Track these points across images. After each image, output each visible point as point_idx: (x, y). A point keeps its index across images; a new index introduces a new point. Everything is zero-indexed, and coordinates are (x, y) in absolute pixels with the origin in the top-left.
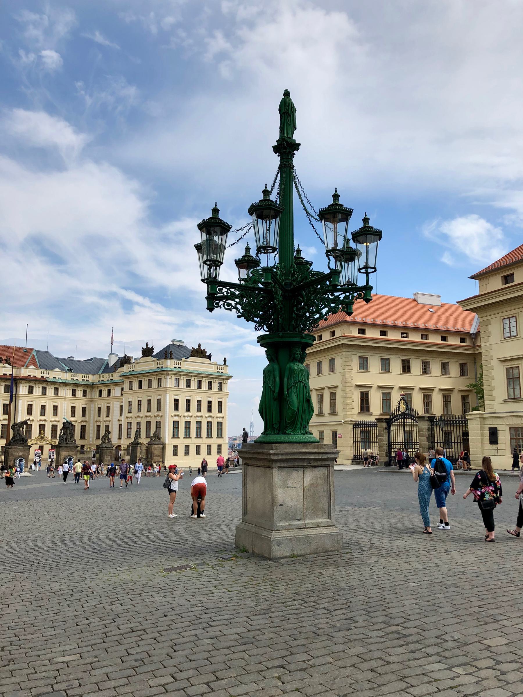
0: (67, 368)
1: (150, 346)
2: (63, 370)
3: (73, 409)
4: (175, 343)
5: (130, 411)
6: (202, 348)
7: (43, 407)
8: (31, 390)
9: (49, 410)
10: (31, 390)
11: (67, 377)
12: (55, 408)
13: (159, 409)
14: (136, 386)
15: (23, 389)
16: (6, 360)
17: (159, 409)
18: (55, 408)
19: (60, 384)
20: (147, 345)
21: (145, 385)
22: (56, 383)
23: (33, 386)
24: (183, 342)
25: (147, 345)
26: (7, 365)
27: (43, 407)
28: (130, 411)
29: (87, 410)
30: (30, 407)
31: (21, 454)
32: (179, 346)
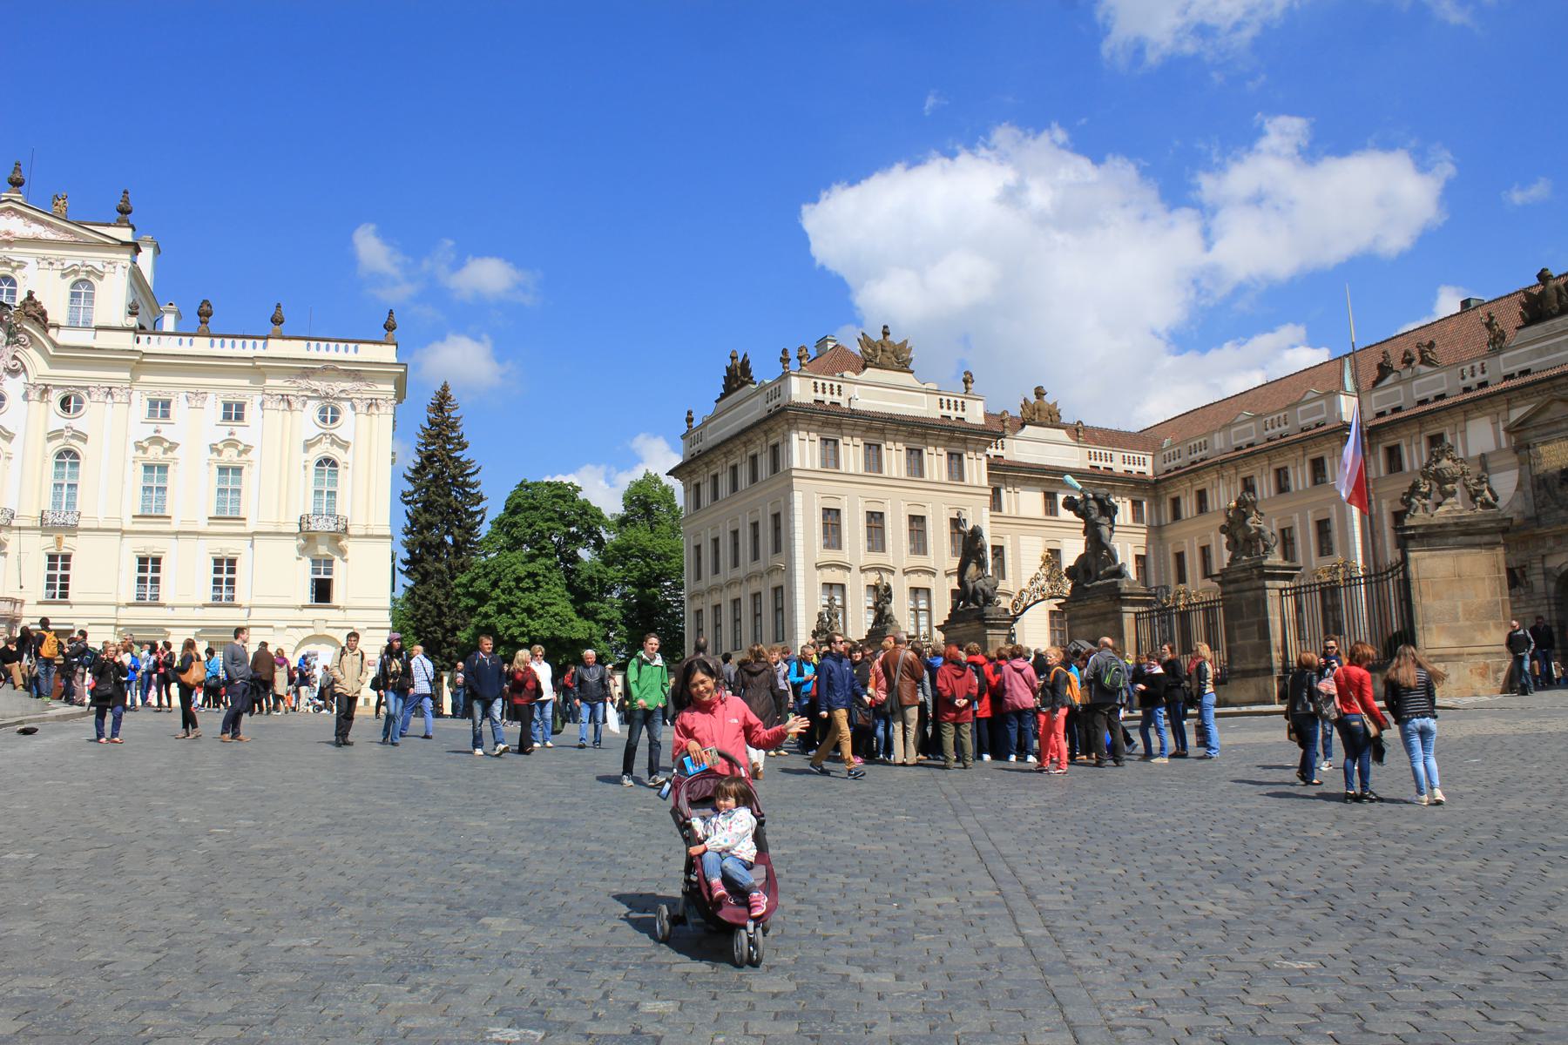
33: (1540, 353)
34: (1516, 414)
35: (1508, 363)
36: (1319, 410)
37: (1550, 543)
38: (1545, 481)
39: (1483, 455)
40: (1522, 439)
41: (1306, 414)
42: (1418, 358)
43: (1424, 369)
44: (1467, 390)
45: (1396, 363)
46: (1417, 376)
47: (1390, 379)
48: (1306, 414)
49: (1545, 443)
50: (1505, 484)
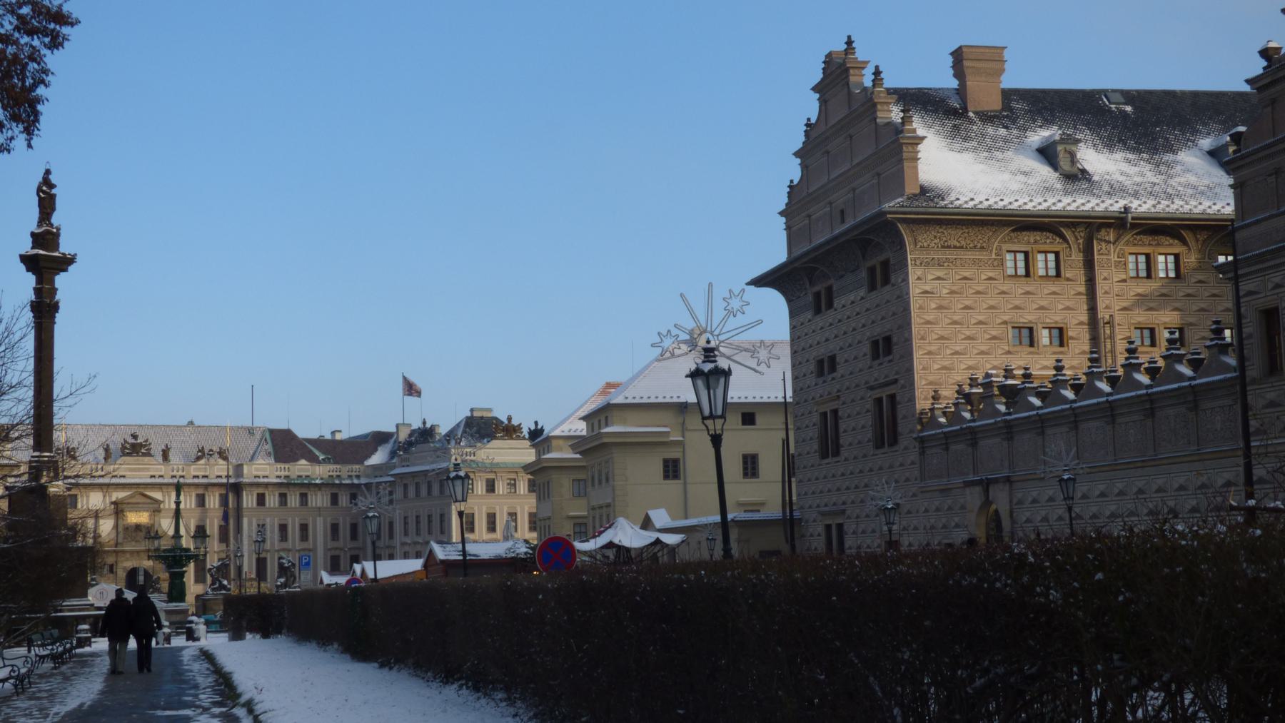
0: (322, 457)
1: (428, 426)
2: (313, 460)
3: (335, 528)
4: (475, 414)
5: (406, 534)
6: (515, 422)
7: (283, 528)
8: (261, 500)
9: (294, 532)
10: (261, 500)
11: (320, 472)
12: (304, 528)
13: (442, 532)
14: (412, 492)
15: (249, 500)
16: (220, 453)
17: (442, 532)
18: (304, 528)
19: (309, 485)
20: (424, 423)
21: (412, 492)
22: (302, 485)
23: (263, 495)
24: (490, 410)
25: (424, 423)
27: (283, 528)
28: (406, 534)
29: (360, 529)
32: (482, 418)
40: (118, 509)
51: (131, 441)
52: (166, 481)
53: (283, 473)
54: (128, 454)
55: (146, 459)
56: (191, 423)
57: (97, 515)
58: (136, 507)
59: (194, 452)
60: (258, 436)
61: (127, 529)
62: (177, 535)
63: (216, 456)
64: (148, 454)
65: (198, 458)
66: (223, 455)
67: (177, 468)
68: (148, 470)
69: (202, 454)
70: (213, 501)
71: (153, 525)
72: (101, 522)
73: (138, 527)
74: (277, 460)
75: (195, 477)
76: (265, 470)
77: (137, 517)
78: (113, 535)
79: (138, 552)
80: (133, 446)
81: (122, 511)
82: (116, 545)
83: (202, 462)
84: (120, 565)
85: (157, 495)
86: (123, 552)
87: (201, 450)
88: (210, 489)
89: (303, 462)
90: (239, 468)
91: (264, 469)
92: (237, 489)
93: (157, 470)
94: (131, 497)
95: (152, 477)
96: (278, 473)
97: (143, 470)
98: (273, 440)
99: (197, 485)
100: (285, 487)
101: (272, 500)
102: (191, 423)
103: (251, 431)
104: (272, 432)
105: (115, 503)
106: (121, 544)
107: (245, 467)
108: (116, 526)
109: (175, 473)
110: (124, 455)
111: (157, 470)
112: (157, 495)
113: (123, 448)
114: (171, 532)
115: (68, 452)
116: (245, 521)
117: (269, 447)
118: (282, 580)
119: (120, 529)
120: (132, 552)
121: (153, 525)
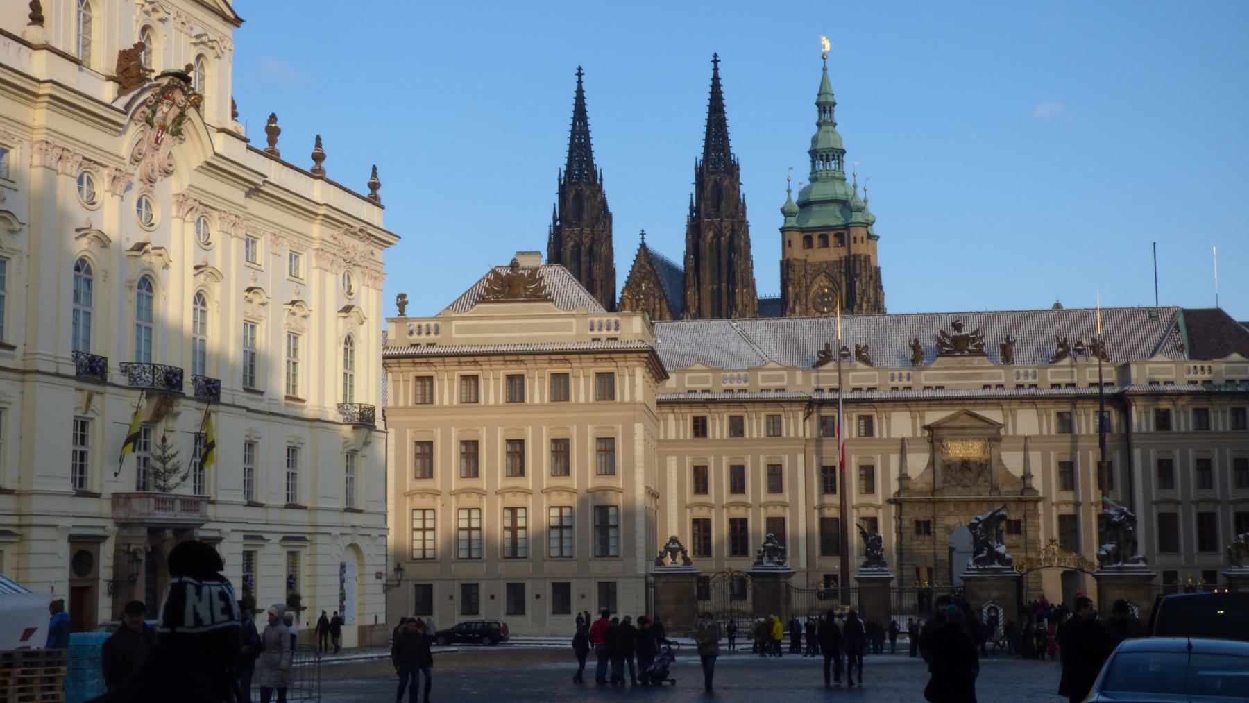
7: (1204, 465)
8: (1163, 421)
26: (1095, 360)
27: (1204, 465)
30: (1165, 469)
31: (995, 594)
33: (951, 377)
34: (933, 416)
35: (927, 377)
36: (781, 378)
37: (951, 508)
38: (949, 466)
39: (903, 439)
40: (935, 436)
41: (764, 379)
42: (853, 354)
43: (860, 365)
44: (896, 388)
45: (835, 351)
46: (855, 370)
47: (830, 365)
48: (764, 379)
49: (952, 440)
50: (918, 463)
51: (952, 333)
52: (1006, 392)
53: (1200, 377)
54: (949, 354)
55: (977, 360)
56: (1058, 306)
57: (903, 447)
58: (961, 433)
59: (1054, 349)
60: (1165, 321)
61: (948, 466)
62: (1027, 476)
63: (1089, 351)
64: (979, 352)
65: (1059, 357)
66: (1097, 349)
67: (1025, 371)
68: (979, 376)
69: (1064, 350)
70: (1087, 423)
71: (989, 462)
72: (909, 457)
73: (965, 464)
74: (1193, 356)
75: (1053, 386)
76: (1168, 371)
77: (958, 450)
78: (929, 478)
79: (967, 503)
80: (955, 340)
81: (941, 441)
82: (934, 491)
83: (1066, 361)
84: (939, 521)
85: (995, 415)
86: (943, 502)
87: (1063, 344)
88: (1079, 404)
89: (1236, 356)
90: (1124, 370)
91: (1175, 371)
92: (1122, 402)
93: (993, 376)
94: (952, 418)
95: (985, 387)
96: (1192, 376)
97: (965, 377)
98: (1188, 326)
99: (1057, 399)
100: (1207, 395)
101: (1183, 421)
102: (1058, 306)
103: (1152, 314)
104: (1188, 313)
105: (928, 428)
106: (941, 490)
107: (1133, 368)
108: (932, 464)
109: (1022, 380)
110: (942, 354)
111: (993, 376)
112: (995, 415)
113: (941, 344)
114: (1018, 472)
115: (858, 353)
116: (1137, 454)
117: (1182, 337)
118: (1110, 547)
119: (938, 468)
120: (957, 503)
121: (989, 462)
